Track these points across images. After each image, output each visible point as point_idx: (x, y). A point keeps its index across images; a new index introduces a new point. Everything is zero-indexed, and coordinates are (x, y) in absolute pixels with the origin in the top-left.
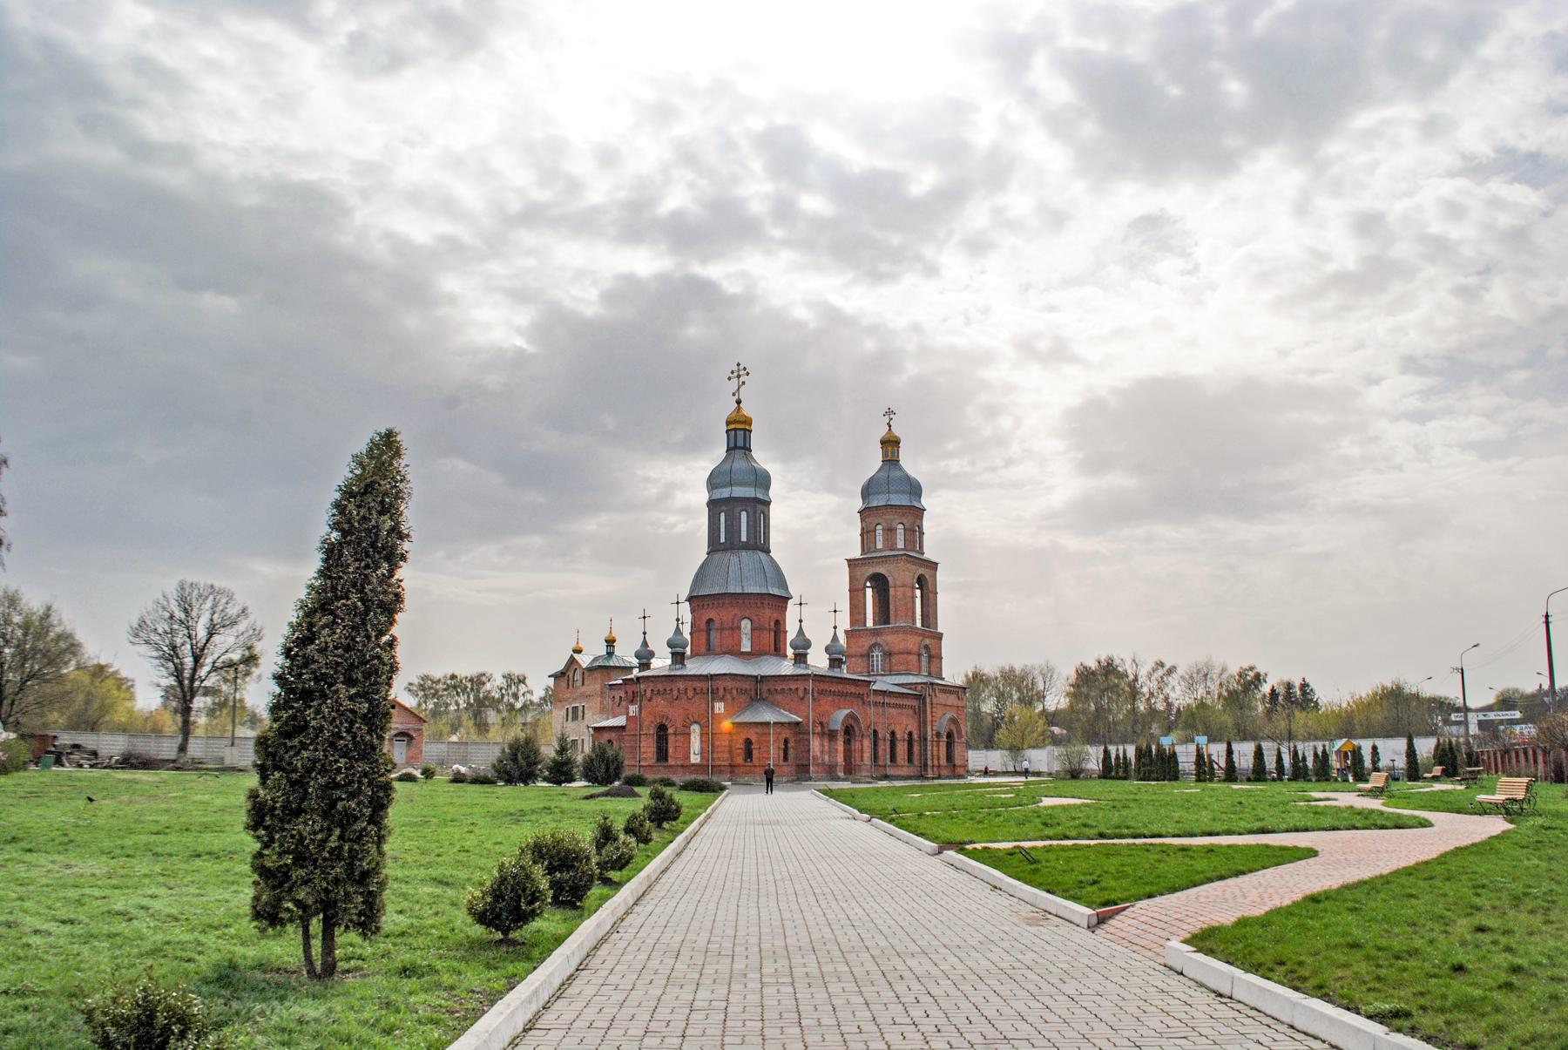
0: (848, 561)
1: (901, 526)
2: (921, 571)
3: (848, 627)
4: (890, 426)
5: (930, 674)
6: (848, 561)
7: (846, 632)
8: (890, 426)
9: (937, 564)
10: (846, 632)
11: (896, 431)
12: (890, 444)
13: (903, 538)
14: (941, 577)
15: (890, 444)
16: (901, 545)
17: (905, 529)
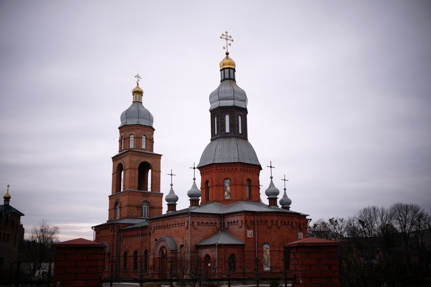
0: (113, 158)
1: (132, 136)
2: (143, 160)
3: (111, 194)
4: (138, 84)
5: (144, 217)
6: (113, 158)
7: (110, 197)
8: (138, 84)
9: (161, 155)
10: (110, 197)
11: (142, 87)
12: (138, 93)
13: (133, 142)
14: (163, 161)
15: (138, 93)
16: (132, 146)
17: (134, 138)
